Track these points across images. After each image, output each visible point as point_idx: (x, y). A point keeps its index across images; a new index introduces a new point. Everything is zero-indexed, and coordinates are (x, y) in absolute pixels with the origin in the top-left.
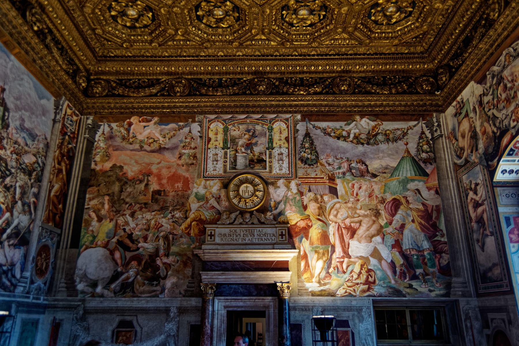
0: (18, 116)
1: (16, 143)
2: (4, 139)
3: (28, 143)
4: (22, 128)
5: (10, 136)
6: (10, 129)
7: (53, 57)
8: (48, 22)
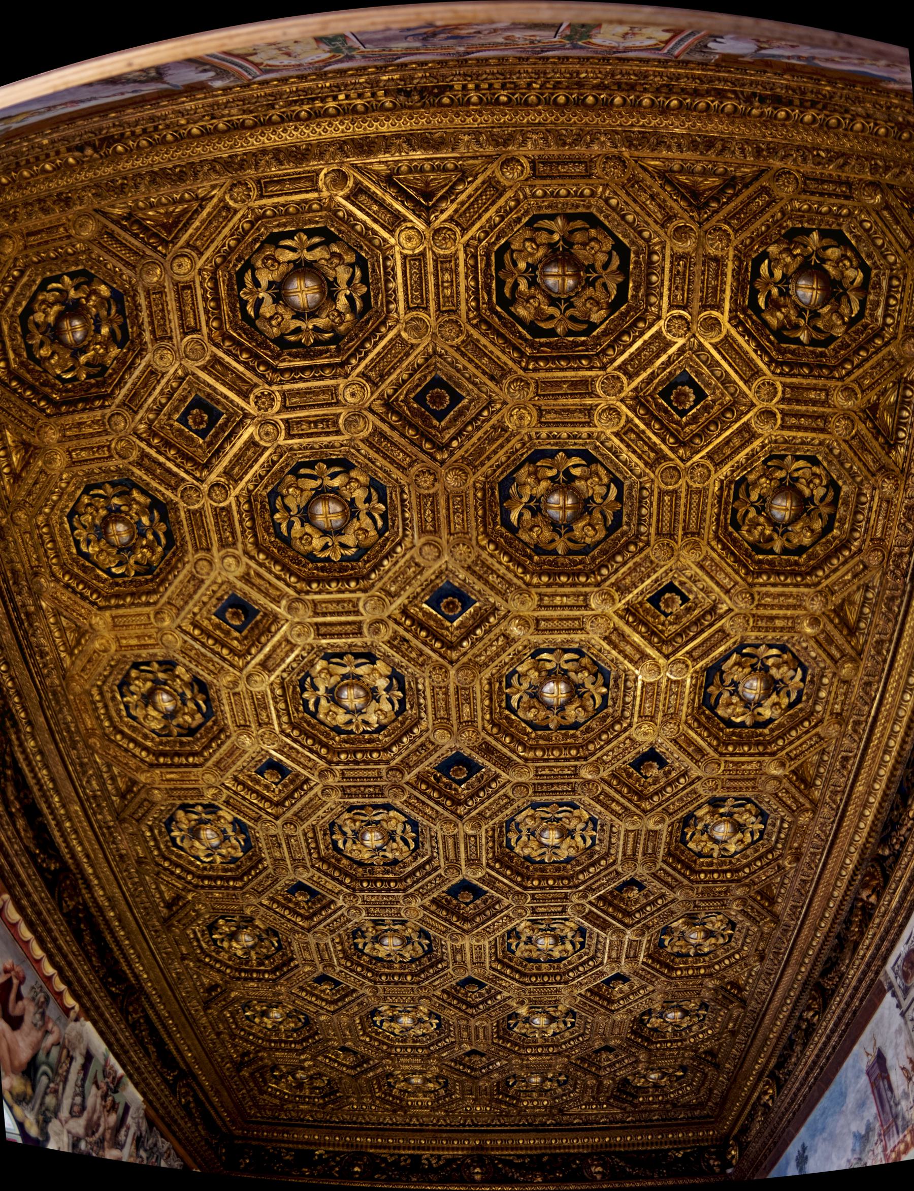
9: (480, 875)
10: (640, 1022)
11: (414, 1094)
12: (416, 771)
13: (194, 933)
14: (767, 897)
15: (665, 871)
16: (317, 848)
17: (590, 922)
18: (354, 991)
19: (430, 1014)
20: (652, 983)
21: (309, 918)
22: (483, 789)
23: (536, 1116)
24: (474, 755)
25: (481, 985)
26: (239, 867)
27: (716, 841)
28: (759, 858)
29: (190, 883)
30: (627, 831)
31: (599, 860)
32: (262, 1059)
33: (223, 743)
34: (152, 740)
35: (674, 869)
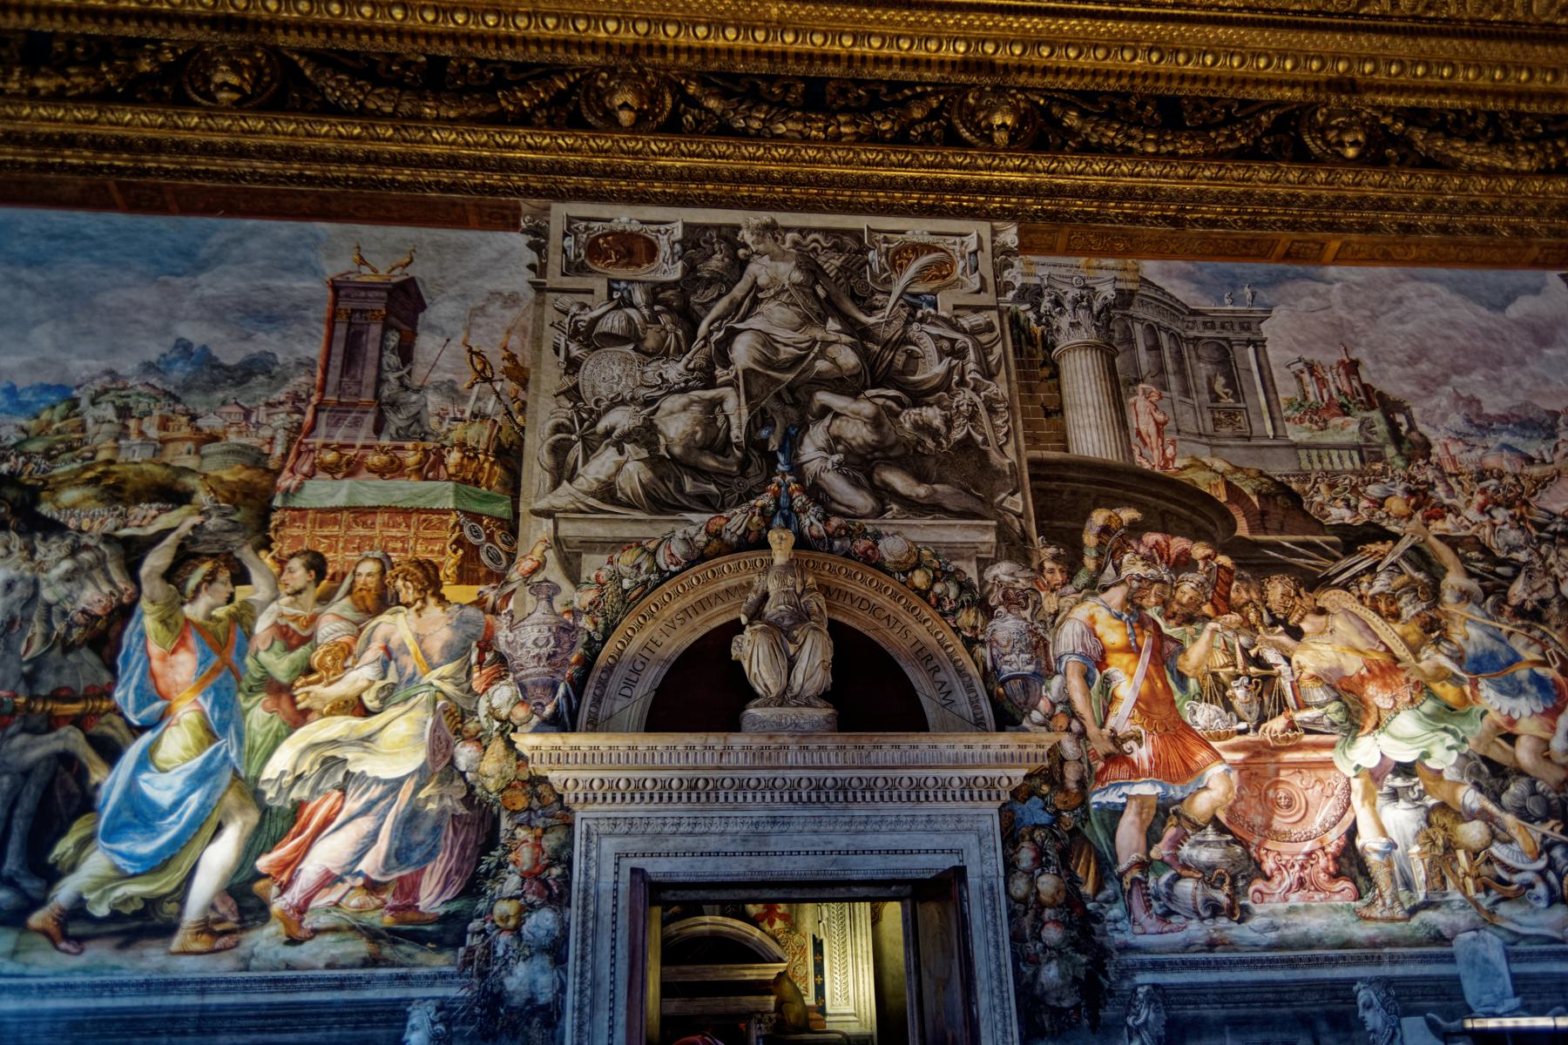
0: (1444, 402)
1: (1482, 475)
2: (1432, 486)
3: (1533, 453)
4: (1481, 424)
5: (1449, 468)
6: (1437, 449)
7: (1472, 170)
8: (1390, 100)
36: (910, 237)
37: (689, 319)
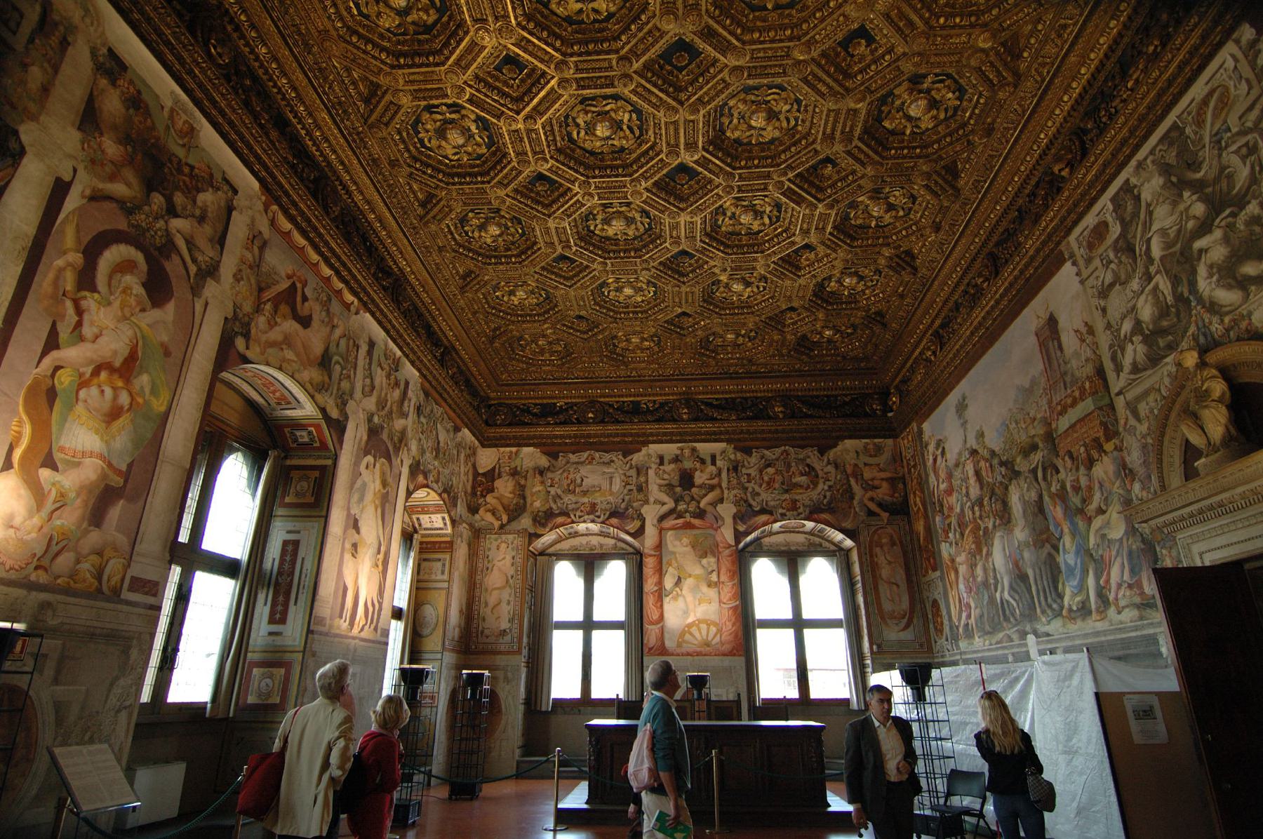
9: (696, 157)
10: (821, 286)
11: (633, 351)
12: (642, 60)
13: (448, 226)
14: (952, 171)
15: (859, 148)
16: (554, 140)
17: (788, 198)
18: (587, 267)
19: (649, 282)
20: (835, 251)
21: (550, 205)
22: (702, 75)
23: (732, 365)
24: (697, 40)
25: (692, 256)
26: (484, 162)
27: (909, 118)
28: (950, 135)
29: (441, 181)
30: (829, 111)
31: (800, 141)
32: (511, 331)
33: (462, 40)
34: (389, 40)
35: (868, 146)
36: (1199, 98)
37: (1131, 250)
